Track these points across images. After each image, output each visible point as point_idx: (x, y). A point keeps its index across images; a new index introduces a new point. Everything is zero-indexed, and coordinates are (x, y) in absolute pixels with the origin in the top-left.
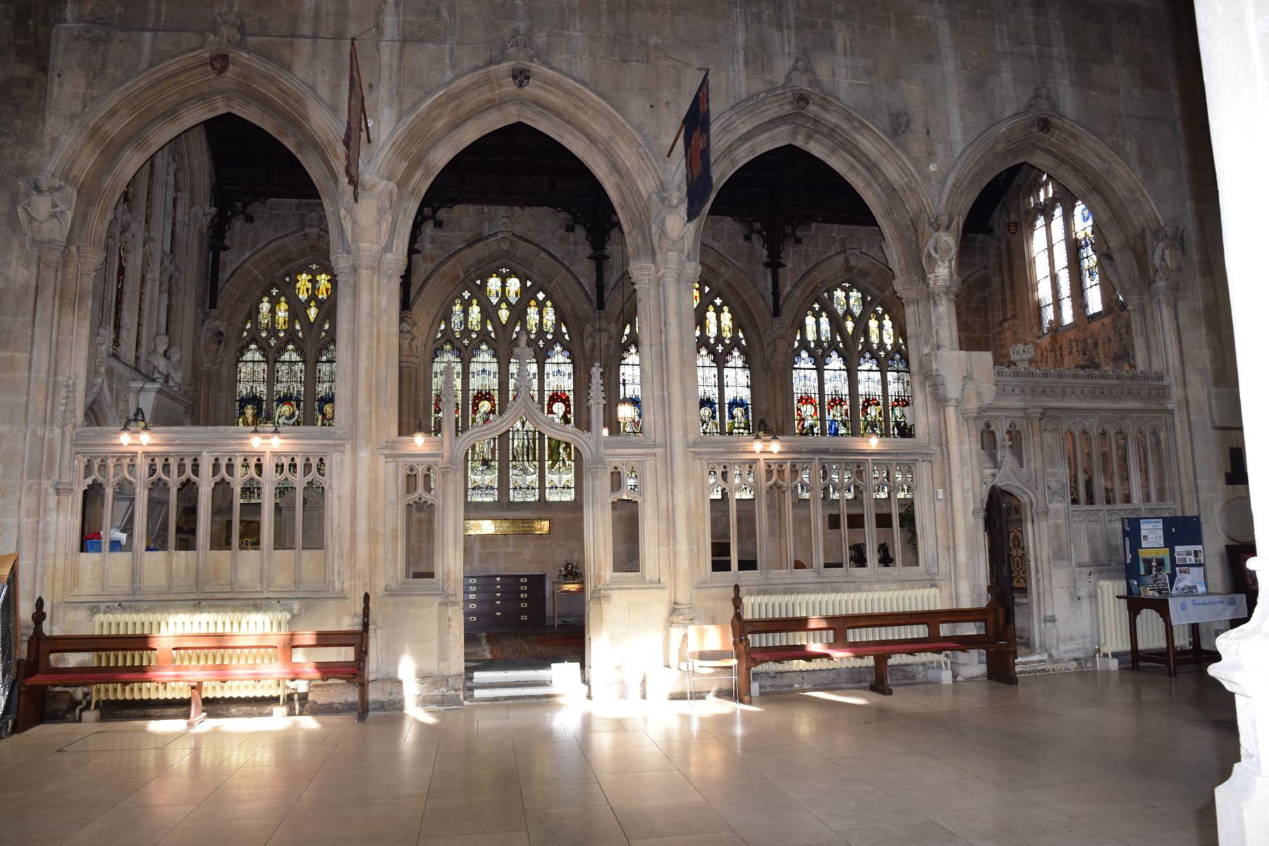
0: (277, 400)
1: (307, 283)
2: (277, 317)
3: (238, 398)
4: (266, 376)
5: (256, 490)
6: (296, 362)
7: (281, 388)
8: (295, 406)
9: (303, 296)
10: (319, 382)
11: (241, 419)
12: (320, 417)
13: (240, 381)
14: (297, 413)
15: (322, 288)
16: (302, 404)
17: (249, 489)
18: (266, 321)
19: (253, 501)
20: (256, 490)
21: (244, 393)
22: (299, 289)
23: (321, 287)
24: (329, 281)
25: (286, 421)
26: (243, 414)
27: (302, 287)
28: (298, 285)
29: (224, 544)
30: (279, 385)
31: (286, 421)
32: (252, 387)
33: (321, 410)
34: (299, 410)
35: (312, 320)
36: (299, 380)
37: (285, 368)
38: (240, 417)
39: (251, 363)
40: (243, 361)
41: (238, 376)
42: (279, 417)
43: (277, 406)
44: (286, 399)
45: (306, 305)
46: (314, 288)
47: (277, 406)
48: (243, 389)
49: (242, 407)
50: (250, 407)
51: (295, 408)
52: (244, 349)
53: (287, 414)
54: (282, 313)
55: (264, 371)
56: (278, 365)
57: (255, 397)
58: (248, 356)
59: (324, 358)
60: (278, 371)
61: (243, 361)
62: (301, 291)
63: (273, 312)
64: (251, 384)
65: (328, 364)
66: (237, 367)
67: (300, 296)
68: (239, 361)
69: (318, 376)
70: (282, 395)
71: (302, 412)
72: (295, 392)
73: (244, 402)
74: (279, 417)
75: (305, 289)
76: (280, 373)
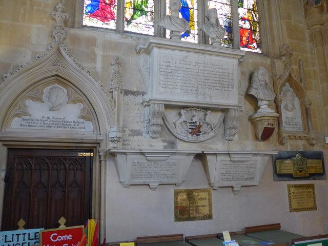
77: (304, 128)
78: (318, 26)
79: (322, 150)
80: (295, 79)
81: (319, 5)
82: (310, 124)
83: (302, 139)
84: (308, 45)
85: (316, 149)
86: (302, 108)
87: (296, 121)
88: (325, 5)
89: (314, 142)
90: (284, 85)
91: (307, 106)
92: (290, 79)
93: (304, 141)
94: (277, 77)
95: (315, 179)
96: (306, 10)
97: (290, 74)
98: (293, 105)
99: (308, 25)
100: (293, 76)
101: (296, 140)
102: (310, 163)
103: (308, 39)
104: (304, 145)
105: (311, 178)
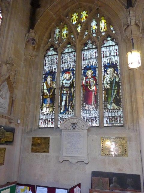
0: (62, 72)
1: (76, 17)
2: (63, 34)
3: (44, 73)
4: (57, 61)
5: (51, 120)
6: (72, 52)
7: (64, 66)
8: (71, 73)
9: (74, 22)
10: (83, 60)
11: (45, 84)
12: (85, 78)
13: (45, 65)
14: (72, 77)
15: (84, 17)
16: (75, 72)
17: (47, 119)
18: (58, 37)
19: (49, 126)
20: (51, 120)
21: (47, 70)
22: (73, 20)
23: (83, 17)
24: (87, 13)
25: (67, 82)
26: (46, 80)
27: (74, 19)
28: (72, 19)
29: (30, 151)
30: (63, 64)
31: (67, 82)
32: (51, 67)
33: (85, 74)
34: (73, 75)
35: (79, 32)
36: (73, 60)
37: (66, 56)
38: (44, 82)
39: (51, 56)
40: (47, 56)
41: (45, 63)
42: (63, 80)
43: (62, 75)
44: (65, 71)
45: (76, 26)
46: (79, 18)
47: (62, 75)
48: (47, 69)
49: (46, 77)
50: (49, 77)
51: (71, 75)
52: (48, 50)
53: (67, 78)
54: (65, 32)
55: (56, 59)
56: (63, 55)
57: (52, 71)
58: (50, 53)
59: (86, 48)
60: (63, 58)
61: (47, 56)
62: (74, 21)
63: (60, 32)
64: (50, 66)
65: (88, 51)
66: (44, 58)
67: (73, 23)
68: (45, 56)
69: (83, 57)
70: (65, 69)
71: (75, 76)
72: (71, 67)
73: (46, 75)
74: (63, 80)
75: (75, 19)
76: (64, 59)
77: (8, 112)
78: (30, 56)
79: (14, 127)
80: (11, 80)
81: (33, 46)
82: (12, 110)
83: (6, 118)
84: (22, 64)
85: (12, 126)
86: (10, 99)
87: (5, 106)
88: (36, 48)
89: (12, 121)
90: (3, 81)
91: (14, 99)
92: (9, 78)
93: (6, 119)
94: (2, 75)
95: (7, 145)
96: (26, 45)
97: (9, 77)
98: (6, 96)
99: (25, 54)
100: (11, 78)
101: (2, 118)
102: (8, 134)
103: (23, 61)
104: (6, 122)
105: (5, 144)
